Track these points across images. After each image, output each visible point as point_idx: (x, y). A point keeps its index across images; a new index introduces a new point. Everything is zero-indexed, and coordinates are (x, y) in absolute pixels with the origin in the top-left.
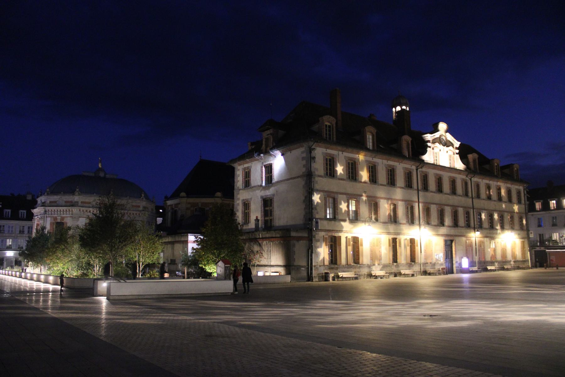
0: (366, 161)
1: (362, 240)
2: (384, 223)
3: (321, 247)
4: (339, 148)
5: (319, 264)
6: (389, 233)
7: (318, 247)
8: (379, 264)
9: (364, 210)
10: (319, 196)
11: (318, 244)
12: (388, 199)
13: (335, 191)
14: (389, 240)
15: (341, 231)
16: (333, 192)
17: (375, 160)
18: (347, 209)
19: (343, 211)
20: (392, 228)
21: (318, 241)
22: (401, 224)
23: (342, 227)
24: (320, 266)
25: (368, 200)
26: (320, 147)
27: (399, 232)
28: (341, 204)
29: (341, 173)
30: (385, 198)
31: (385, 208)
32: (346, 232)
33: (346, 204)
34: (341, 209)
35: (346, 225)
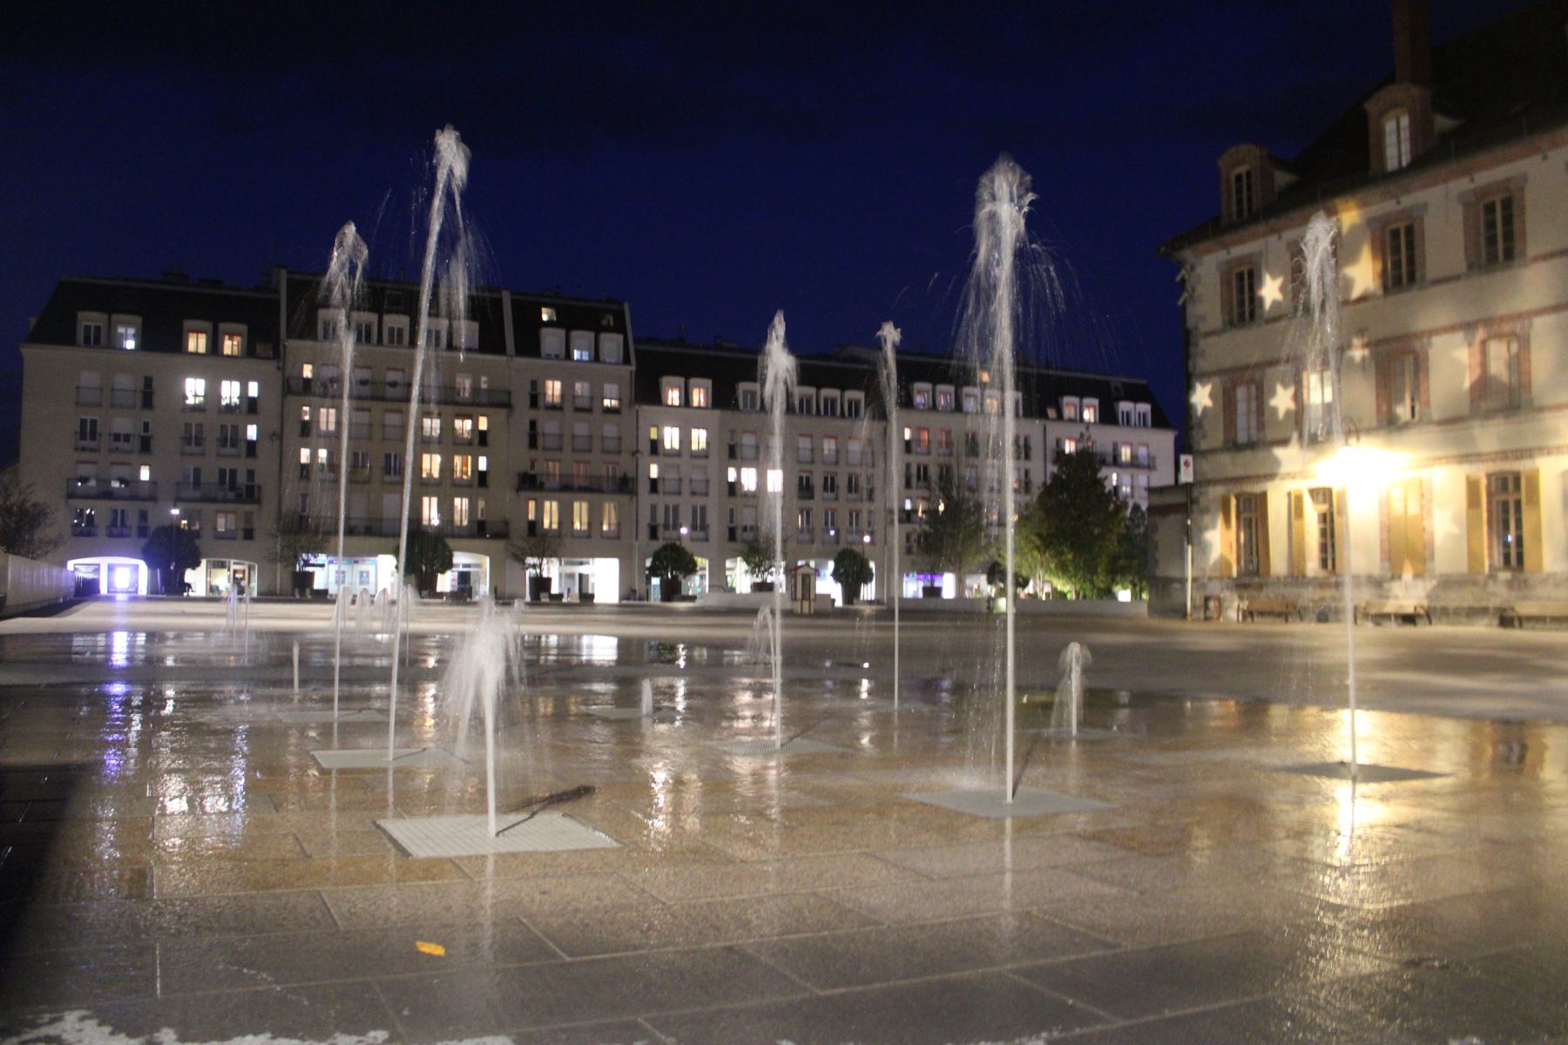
0: (1370, 222)
1: (1342, 495)
2: (1451, 421)
3: (1214, 526)
4: (1260, 228)
5: (1209, 573)
6: (1465, 458)
7: (1207, 528)
8: (1417, 576)
9: (1364, 394)
10: (1208, 388)
11: (1207, 519)
12: (1469, 327)
13: (1255, 359)
14: (1472, 486)
15: (1271, 476)
16: (1247, 367)
17: (1408, 201)
18: (1292, 405)
19: (1281, 414)
20: (1488, 436)
21: (1205, 511)
22: (1541, 409)
23: (1276, 462)
24: (1210, 579)
25: (1375, 356)
26: (1209, 251)
27: (1531, 443)
28: (1273, 393)
29: (1275, 303)
30: (1452, 329)
31: (1454, 362)
32: (1292, 476)
33: (1291, 391)
34: (1275, 410)
35: (1288, 456)
